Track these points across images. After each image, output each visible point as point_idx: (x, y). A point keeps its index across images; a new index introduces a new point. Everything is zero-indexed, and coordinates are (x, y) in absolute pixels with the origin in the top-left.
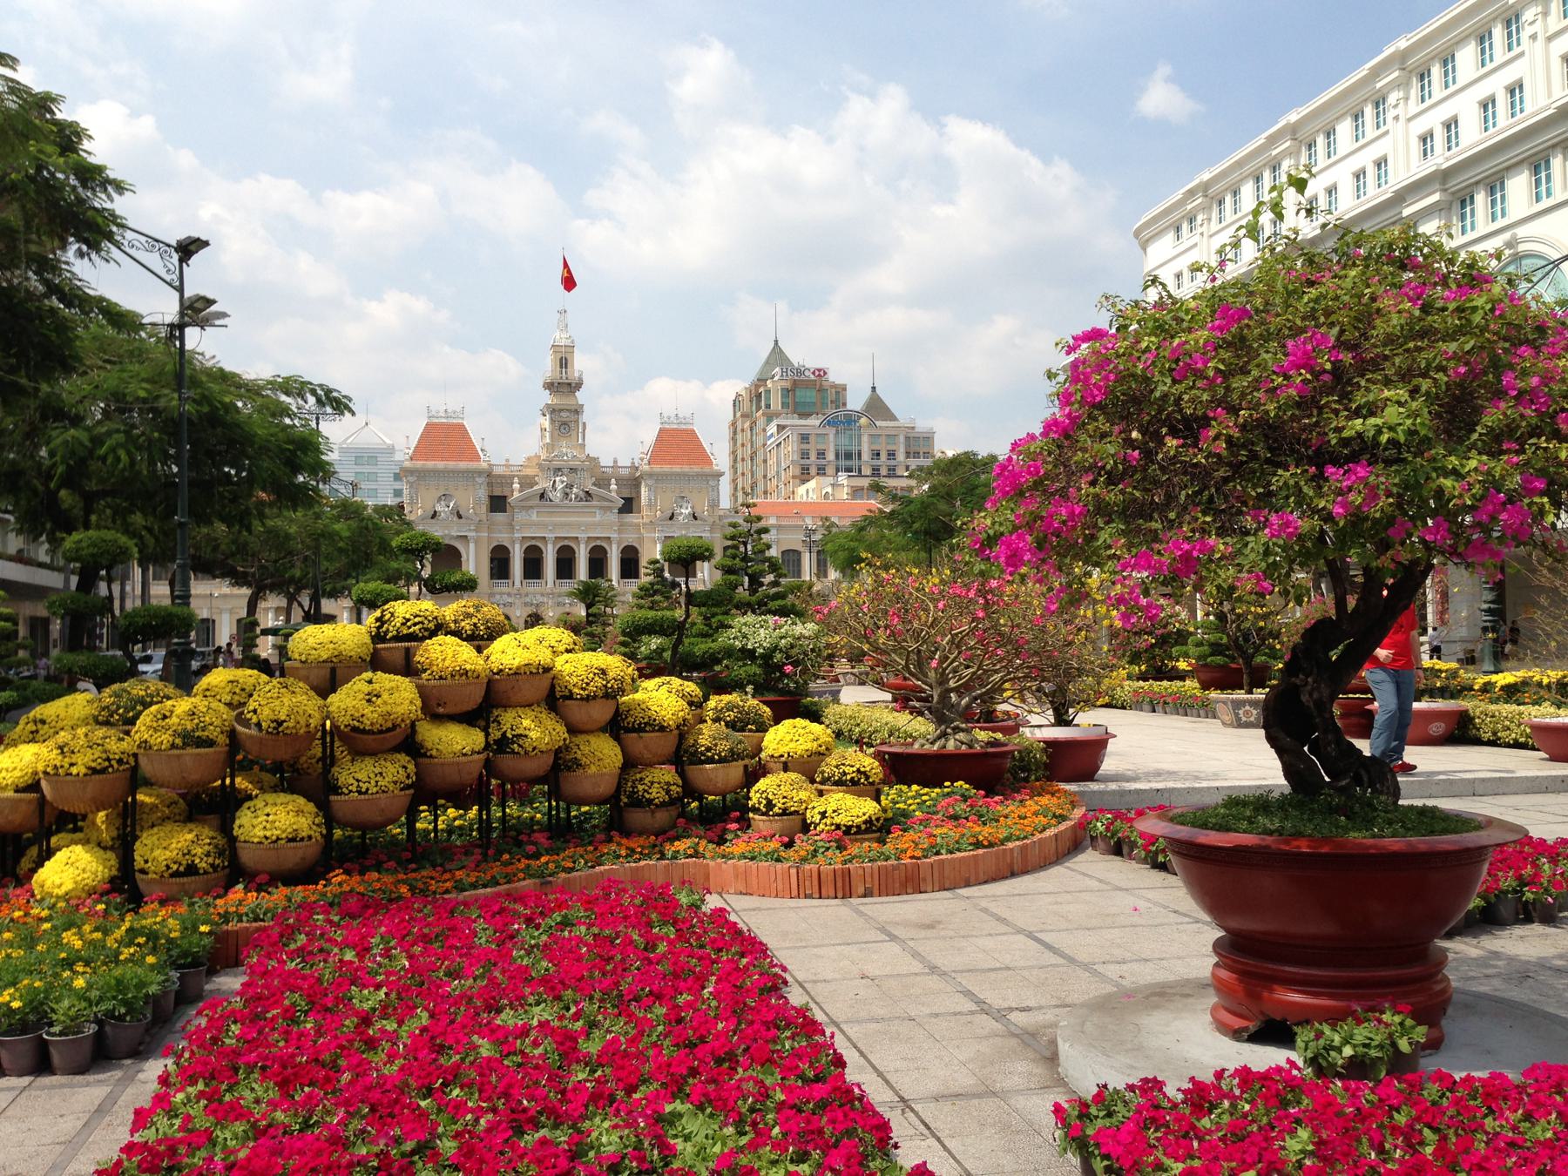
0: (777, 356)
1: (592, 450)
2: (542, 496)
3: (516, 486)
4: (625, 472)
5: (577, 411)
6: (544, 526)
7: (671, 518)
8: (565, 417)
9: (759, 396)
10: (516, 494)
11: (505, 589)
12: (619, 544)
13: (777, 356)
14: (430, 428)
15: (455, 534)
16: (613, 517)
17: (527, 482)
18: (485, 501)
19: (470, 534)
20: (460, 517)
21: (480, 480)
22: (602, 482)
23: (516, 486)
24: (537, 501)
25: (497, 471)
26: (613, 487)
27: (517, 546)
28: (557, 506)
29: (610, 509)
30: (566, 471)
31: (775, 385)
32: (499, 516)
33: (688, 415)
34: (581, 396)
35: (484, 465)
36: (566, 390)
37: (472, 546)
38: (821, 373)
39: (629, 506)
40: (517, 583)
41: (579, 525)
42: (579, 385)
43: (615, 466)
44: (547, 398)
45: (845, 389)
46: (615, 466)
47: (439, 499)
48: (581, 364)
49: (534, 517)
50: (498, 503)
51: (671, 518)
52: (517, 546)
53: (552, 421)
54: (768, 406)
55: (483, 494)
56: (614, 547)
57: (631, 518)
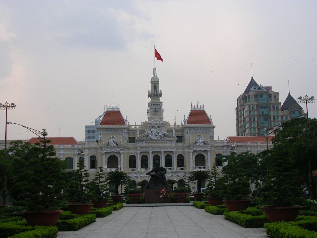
0: (253, 83)
1: (166, 119)
2: (147, 137)
3: (138, 133)
4: (179, 127)
5: (160, 105)
6: (148, 148)
7: (195, 144)
8: (155, 108)
9: (246, 98)
10: (138, 136)
11: (134, 171)
13: (253, 83)
14: (107, 112)
16: (174, 144)
17: (142, 131)
18: (127, 139)
22: (170, 131)
23: (138, 133)
24: (145, 139)
25: (131, 127)
26: (174, 133)
27: (139, 155)
30: (156, 127)
31: (252, 93)
32: (132, 145)
34: (161, 99)
35: (125, 126)
37: (122, 155)
38: (269, 88)
39: (180, 139)
42: (161, 96)
44: (149, 100)
45: (278, 94)
47: (110, 138)
48: (161, 87)
50: (132, 140)
52: (139, 155)
53: (151, 109)
54: (249, 101)
55: (126, 136)
56: (174, 155)
57: (180, 144)
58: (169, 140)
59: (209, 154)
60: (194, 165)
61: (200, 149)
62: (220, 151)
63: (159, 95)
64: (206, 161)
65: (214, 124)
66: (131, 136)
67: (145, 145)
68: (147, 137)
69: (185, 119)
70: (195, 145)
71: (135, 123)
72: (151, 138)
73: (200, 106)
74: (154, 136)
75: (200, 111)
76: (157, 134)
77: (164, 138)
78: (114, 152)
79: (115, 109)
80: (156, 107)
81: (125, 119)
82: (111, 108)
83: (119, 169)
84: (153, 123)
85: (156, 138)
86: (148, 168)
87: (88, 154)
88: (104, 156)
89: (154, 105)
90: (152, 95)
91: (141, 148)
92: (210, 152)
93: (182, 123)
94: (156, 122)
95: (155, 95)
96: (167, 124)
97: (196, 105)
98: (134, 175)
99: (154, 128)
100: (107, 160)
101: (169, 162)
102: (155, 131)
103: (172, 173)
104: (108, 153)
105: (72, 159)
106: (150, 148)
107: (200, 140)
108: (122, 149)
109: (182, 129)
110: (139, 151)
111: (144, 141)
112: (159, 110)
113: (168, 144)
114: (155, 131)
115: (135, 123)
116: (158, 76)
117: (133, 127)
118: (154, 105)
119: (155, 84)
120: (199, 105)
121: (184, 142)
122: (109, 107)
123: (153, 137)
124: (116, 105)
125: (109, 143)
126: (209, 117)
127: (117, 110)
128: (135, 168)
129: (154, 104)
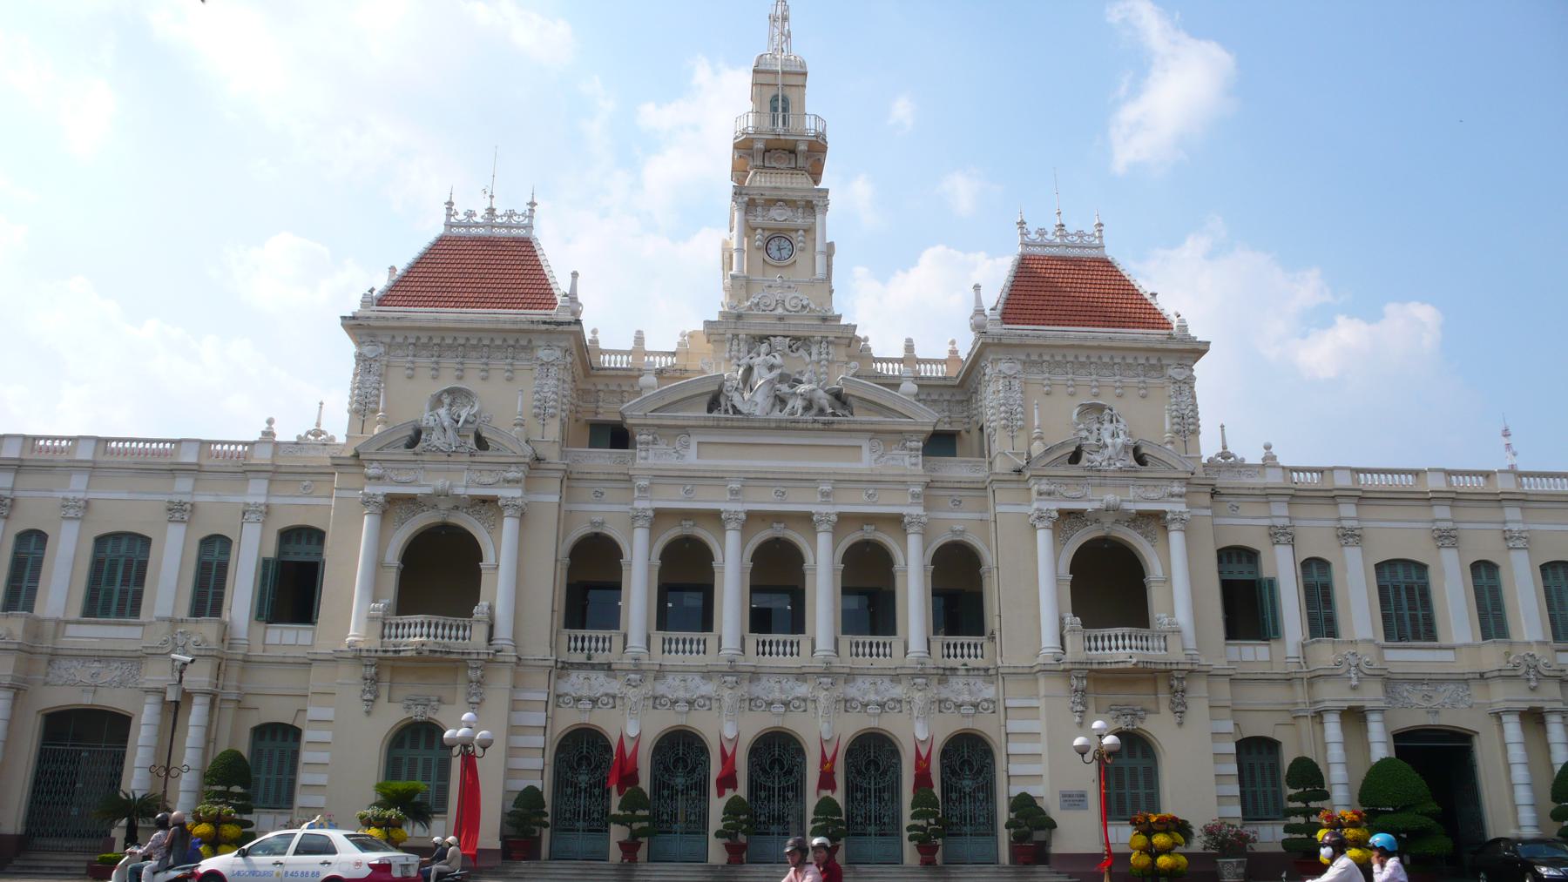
2: (714, 404)
3: (649, 380)
4: (937, 371)
5: (813, 205)
7: (1075, 458)
12: (925, 534)
16: (908, 462)
20: (481, 443)
21: (543, 354)
23: (649, 380)
27: (640, 537)
28: (744, 424)
29: (899, 436)
33: (1089, 229)
37: (509, 525)
40: (636, 641)
41: (806, 480)
43: (909, 358)
46: (909, 358)
51: (1075, 458)
53: (749, 229)
56: (914, 542)
57: (955, 469)
58: (876, 433)
59: (1176, 539)
60: (1073, 621)
61: (1111, 497)
62: (1246, 527)
63: (802, 147)
64: (1155, 596)
65: (1197, 332)
66: (600, 417)
67: (691, 457)
68: (710, 410)
69: (979, 311)
70: (1074, 470)
71: (639, 338)
72: (740, 412)
73: (1080, 234)
75: (1077, 262)
76: (785, 388)
77: (834, 414)
78: (459, 504)
79: (501, 226)
80: (779, 215)
81: (561, 285)
82: (478, 219)
83: (479, 634)
84: (763, 317)
85: (784, 415)
86: (711, 638)
87: (267, 511)
89: (771, 203)
90: (760, 145)
91: (660, 477)
92: (1187, 528)
93: (954, 352)
94: (780, 311)
95: (781, 164)
96: (849, 342)
97: (1051, 228)
98: (600, 684)
99: (764, 348)
100: (393, 556)
101: (870, 605)
102: (771, 368)
103: (896, 678)
104: (411, 499)
105: (146, 541)
106: (726, 484)
107: (1109, 441)
108: (510, 475)
109: (962, 386)
110: (645, 505)
111: (684, 430)
112: (798, 238)
113: (867, 460)
114: (771, 368)
115: (639, 338)
116: (802, 49)
117: (622, 362)
118: (771, 203)
119: (779, 88)
120: (1070, 229)
121: (982, 451)
122: (461, 217)
123: (755, 402)
124: (509, 202)
125: (418, 433)
126: (1147, 296)
127: (522, 233)
128: (607, 633)
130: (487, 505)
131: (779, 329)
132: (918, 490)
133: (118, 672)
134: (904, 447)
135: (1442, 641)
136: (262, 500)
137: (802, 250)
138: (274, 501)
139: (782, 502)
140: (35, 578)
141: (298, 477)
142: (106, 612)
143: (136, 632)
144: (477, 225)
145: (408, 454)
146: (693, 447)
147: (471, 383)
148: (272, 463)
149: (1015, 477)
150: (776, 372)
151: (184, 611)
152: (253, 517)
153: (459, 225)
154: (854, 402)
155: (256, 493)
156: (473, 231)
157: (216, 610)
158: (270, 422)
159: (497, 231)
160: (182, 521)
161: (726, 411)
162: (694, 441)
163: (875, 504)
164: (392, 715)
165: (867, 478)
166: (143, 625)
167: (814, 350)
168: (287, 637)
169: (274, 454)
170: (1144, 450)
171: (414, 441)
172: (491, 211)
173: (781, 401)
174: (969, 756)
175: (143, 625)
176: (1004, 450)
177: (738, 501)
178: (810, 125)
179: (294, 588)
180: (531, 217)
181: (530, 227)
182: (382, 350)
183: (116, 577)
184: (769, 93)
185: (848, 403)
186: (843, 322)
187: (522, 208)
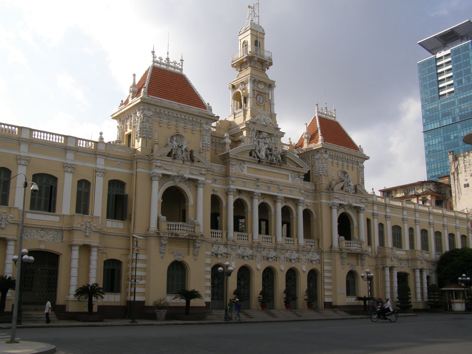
15: (187, 176)
16: (300, 182)
19: (201, 178)
20: (192, 160)
24: (246, 156)
36: (259, 66)
37: (201, 190)
41: (278, 185)
49: (245, 172)
51: (342, 188)
65: (366, 152)
74: (262, 154)
79: (172, 67)
80: (261, 86)
82: (163, 61)
87: (104, 172)
88: (156, 184)
89: (260, 82)
90: (256, 59)
99: (261, 136)
104: (168, 176)
108: (204, 172)
118: (260, 82)
129: (261, 79)
130: (194, 182)
131: (265, 130)
132: (303, 192)
133: (52, 236)
134: (299, 177)
135: (403, 249)
136: (103, 167)
137: (266, 101)
138: (108, 168)
139: (244, 187)
140: (55, 197)
141: (116, 160)
142: (39, 209)
143: (57, 219)
144: (164, 64)
145: (170, 159)
146: (246, 168)
147: (181, 132)
148: (99, 150)
149: (327, 191)
150: (267, 146)
151: (74, 212)
152: (100, 174)
153: (157, 62)
154: (288, 160)
155: (101, 163)
156: (162, 66)
157: (86, 212)
158: (101, 134)
159: (170, 68)
160: (71, 172)
161: (254, 157)
162: (246, 165)
163: (292, 195)
164: (170, 259)
165: (285, 185)
166: (59, 216)
167: (273, 138)
168: (115, 225)
169: (106, 148)
170: (358, 188)
171: (169, 155)
172: (168, 59)
173: (267, 155)
174: (313, 275)
175: (59, 216)
176: (325, 182)
177: (259, 189)
178: (267, 55)
179: (119, 204)
180: (182, 66)
181: (181, 70)
182: (152, 113)
183: (45, 194)
184: (255, 39)
185: (278, 159)
186: (280, 130)
187: (178, 62)
